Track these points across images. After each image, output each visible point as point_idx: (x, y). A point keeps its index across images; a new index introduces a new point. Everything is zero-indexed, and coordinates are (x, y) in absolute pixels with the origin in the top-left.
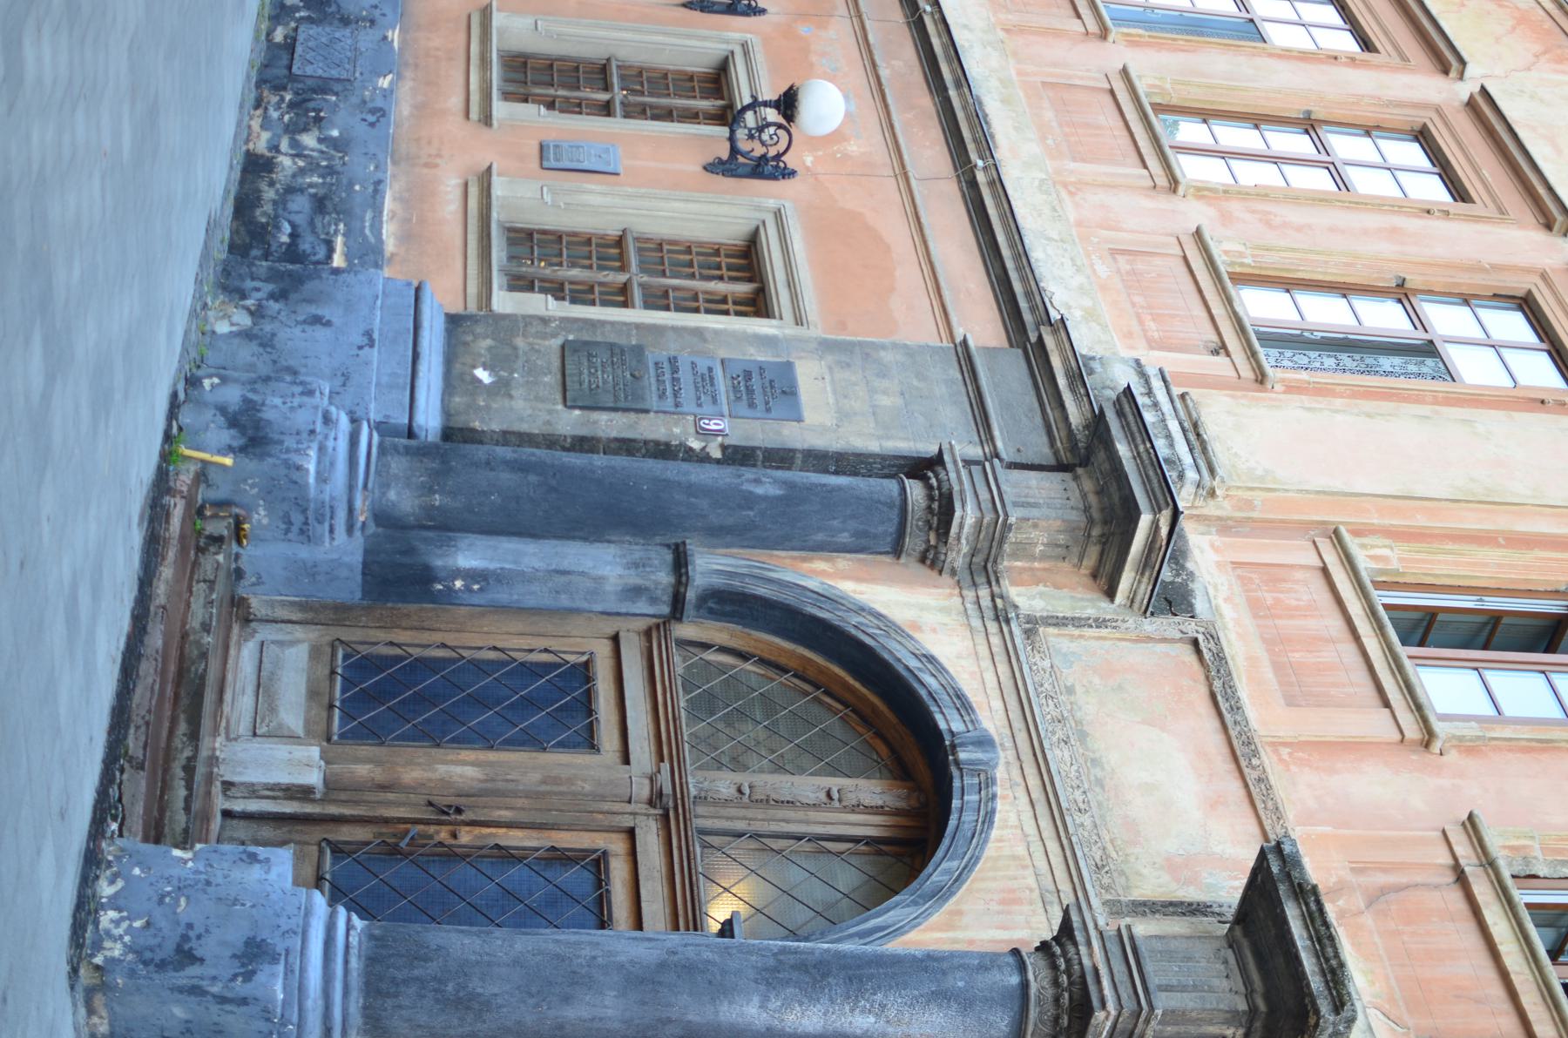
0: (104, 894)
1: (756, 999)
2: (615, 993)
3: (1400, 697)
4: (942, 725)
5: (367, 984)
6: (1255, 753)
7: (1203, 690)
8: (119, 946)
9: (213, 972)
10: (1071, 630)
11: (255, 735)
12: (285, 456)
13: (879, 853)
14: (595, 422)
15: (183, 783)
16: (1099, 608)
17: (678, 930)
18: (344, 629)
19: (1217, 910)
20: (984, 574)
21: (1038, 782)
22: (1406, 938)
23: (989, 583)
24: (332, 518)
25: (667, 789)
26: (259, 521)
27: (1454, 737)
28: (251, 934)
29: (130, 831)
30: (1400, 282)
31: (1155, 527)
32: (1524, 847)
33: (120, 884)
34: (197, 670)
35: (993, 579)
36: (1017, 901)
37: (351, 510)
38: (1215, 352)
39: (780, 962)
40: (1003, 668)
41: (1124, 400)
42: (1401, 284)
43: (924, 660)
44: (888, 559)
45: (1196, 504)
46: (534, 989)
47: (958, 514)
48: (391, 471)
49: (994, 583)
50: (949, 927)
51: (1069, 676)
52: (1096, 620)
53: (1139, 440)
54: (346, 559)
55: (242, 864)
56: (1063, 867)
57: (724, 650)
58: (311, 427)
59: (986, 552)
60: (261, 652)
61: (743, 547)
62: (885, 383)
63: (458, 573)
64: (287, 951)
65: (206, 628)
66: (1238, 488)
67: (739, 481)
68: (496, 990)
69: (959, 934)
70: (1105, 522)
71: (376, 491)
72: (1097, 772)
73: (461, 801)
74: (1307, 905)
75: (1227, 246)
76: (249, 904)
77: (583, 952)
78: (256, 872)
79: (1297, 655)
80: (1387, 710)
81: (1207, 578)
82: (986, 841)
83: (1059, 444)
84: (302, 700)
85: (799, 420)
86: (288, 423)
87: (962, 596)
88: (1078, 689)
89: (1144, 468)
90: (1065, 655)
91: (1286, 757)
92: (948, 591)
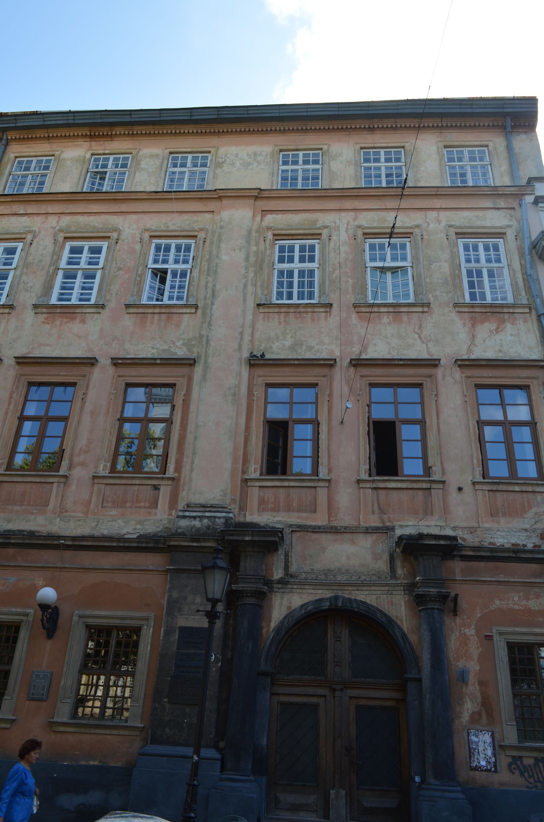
4: (327, 607)
19: (392, 552)
23: (272, 583)
32: (365, 470)
35: (270, 582)
40: (307, 587)
42: (119, 420)
50: (401, 620)
51: (307, 569)
69: (404, 618)
75: (101, 469)
79: (294, 504)
82: (372, 605)
88: (312, 567)
91: (334, 519)
92: (273, 596)
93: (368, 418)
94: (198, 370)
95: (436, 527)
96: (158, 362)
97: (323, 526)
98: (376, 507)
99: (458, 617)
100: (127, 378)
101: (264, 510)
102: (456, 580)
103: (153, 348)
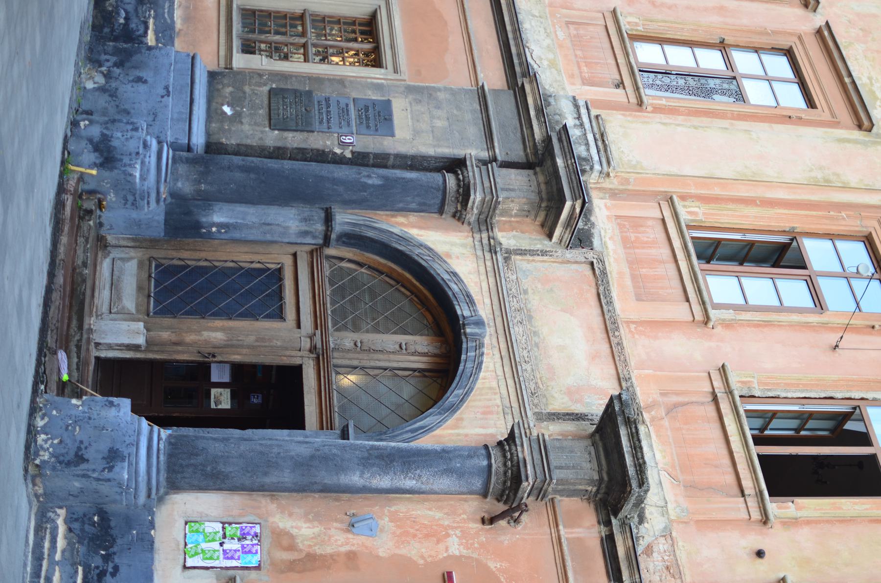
0: (39, 425)
1: (358, 473)
2: (288, 471)
3: (694, 296)
4: (459, 312)
5: (168, 467)
6: (617, 329)
7: (594, 291)
8: (47, 454)
9: (94, 467)
10: (528, 257)
11: (110, 312)
12: (123, 169)
13: (425, 376)
14: (286, 138)
15: (75, 355)
16: (544, 245)
17: (323, 429)
18: (155, 250)
19: (590, 417)
20: (485, 224)
21: (505, 346)
22: (684, 432)
23: (488, 230)
24: (148, 197)
25: (319, 345)
26: (111, 199)
27: (720, 319)
28: (111, 446)
29: (50, 390)
30: (721, 41)
31: (573, 208)
32: (749, 382)
33: (46, 419)
34: (81, 290)
35: (490, 228)
36: (491, 413)
37: (158, 193)
38: (617, 86)
39: (370, 454)
40: (492, 280)
41: (562, 132)
42: (722, 42)
43: (451, 274)
44: (436, 216)
45: (599, 181)
46: (250, 469)
47: (472, 197)
48: (179, 172)
49: (490, 230)
50: (456, 427)
51: (525, 283)
52: (542, 251)
53: (568, 157)
54: (156, 218)
55: (106, 407)
56: (515, 393)
57: (350, 261)
58: (137, 150)
59: (487, 213)
60: (113, 264)
61: (361, 209)
62: (438, 113)
63: (214, 224)
64: (129, 455)
65: (85, 264)
66: (622, 172)
67: (359, 176)
68: (231, 470)
69: (461, 431)
70: (549, 200)
71: (171, 183)
72: (536, 339)
73: (216, 350)
74: (631, 429)
75: (631, 19)
76: (110, 430)
77: (274, 451)
78: (113, 412)
79: (644, 270)
80: (688, 303)
81: (601, 225)
82: (477, 379)
83: (528, 150)
84: (134, 292)
85: (393, 135)
86: (125, 148)
87: (473, 237)
88: (530, 291)
89: (570, 174)
90: (525, 271)
91: (633, 330)
92: (466, 234)
93: (862, 399)
94: (857, 134)
95: (662, 498)
96: (847, 80)
97: (614, 309)
98: (675, 399)
99: (480, 526)
100: (800, 47)
101: (621, 227)
102: (557, 526)
103: (870, 79)
